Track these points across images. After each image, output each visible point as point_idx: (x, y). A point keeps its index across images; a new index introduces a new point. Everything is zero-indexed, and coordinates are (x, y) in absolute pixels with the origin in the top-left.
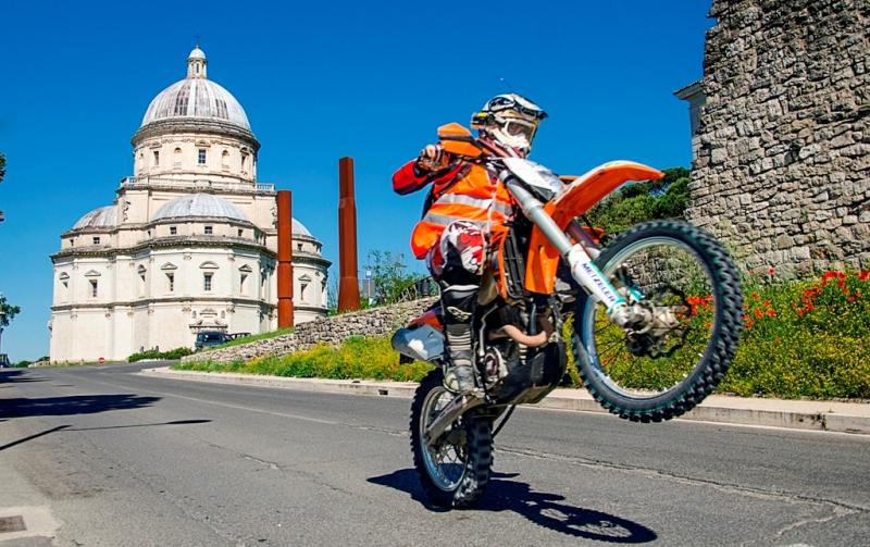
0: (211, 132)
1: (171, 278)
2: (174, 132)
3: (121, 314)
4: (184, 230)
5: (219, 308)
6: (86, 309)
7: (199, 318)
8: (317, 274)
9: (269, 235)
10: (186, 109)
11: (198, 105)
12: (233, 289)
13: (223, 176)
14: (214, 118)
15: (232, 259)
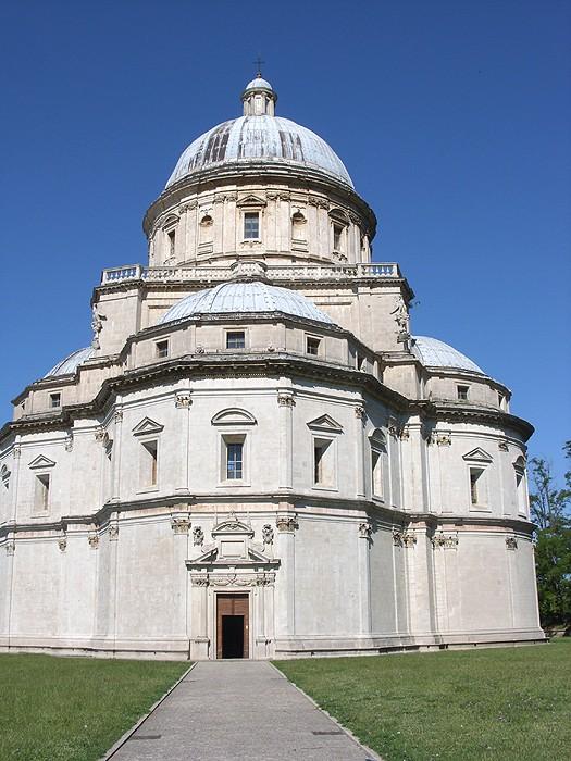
0: (267, 180)
1: (152, 449)
2: (200, 189)
3: (78, 539)
4: (182, 346)
5: (260, 518)
6: (29, 534)
7: (210, 542)
8: (504, 447)
9: (392, 364)
10: (223, 151)
11: (244, 141)
12: (293, 474)
13: (294, 259)
14: (276, 159)
15: (289, 401)
